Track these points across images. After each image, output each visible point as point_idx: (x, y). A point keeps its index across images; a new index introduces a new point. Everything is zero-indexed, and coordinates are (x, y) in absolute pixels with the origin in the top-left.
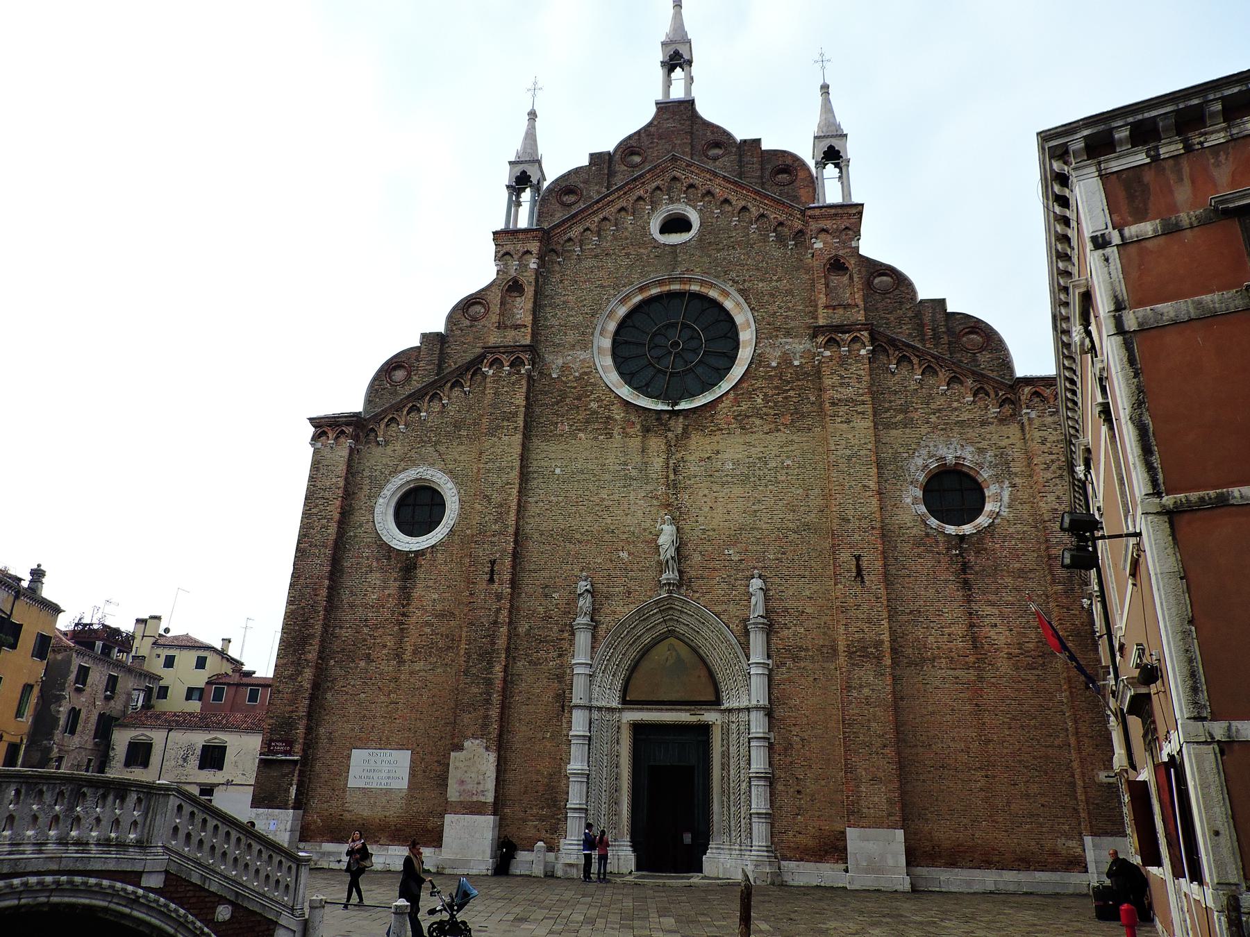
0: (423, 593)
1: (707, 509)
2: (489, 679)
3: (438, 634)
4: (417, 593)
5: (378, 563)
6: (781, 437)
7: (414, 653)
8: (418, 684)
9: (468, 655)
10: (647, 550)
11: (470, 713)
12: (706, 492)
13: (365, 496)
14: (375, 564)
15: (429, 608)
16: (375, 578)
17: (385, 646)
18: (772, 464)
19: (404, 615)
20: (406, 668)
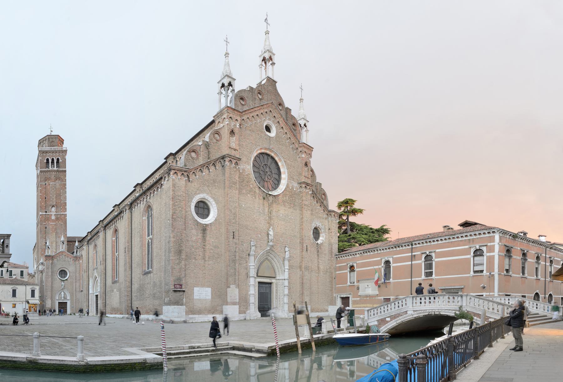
0: (209, 239)
1: (277, 226)
2: (235, 268)
3: (214, 253)
4: (208, 238)
5: (194, 227)
6: (291, 210)
7: (209, 258)
8: (211, 268)
9: (229, 260)
10: (265, 235)
11: (231, 277)
12: (277, 221)
13: (187, 201)
14: (193, 227)
15: (212, 244)
16: (194, 232)
17: (200, 255)
18: (289, 217)
19: (204, 245)
20: (207, 263)
